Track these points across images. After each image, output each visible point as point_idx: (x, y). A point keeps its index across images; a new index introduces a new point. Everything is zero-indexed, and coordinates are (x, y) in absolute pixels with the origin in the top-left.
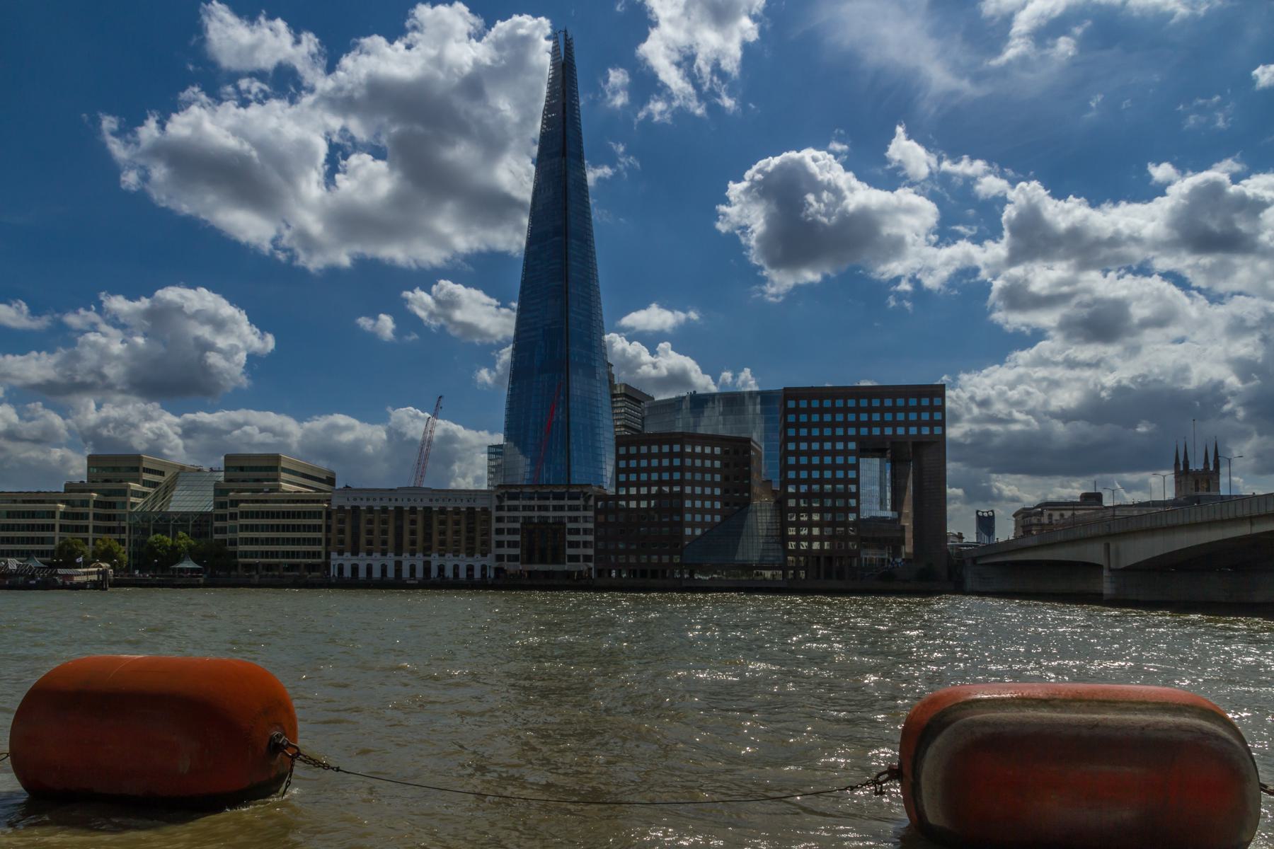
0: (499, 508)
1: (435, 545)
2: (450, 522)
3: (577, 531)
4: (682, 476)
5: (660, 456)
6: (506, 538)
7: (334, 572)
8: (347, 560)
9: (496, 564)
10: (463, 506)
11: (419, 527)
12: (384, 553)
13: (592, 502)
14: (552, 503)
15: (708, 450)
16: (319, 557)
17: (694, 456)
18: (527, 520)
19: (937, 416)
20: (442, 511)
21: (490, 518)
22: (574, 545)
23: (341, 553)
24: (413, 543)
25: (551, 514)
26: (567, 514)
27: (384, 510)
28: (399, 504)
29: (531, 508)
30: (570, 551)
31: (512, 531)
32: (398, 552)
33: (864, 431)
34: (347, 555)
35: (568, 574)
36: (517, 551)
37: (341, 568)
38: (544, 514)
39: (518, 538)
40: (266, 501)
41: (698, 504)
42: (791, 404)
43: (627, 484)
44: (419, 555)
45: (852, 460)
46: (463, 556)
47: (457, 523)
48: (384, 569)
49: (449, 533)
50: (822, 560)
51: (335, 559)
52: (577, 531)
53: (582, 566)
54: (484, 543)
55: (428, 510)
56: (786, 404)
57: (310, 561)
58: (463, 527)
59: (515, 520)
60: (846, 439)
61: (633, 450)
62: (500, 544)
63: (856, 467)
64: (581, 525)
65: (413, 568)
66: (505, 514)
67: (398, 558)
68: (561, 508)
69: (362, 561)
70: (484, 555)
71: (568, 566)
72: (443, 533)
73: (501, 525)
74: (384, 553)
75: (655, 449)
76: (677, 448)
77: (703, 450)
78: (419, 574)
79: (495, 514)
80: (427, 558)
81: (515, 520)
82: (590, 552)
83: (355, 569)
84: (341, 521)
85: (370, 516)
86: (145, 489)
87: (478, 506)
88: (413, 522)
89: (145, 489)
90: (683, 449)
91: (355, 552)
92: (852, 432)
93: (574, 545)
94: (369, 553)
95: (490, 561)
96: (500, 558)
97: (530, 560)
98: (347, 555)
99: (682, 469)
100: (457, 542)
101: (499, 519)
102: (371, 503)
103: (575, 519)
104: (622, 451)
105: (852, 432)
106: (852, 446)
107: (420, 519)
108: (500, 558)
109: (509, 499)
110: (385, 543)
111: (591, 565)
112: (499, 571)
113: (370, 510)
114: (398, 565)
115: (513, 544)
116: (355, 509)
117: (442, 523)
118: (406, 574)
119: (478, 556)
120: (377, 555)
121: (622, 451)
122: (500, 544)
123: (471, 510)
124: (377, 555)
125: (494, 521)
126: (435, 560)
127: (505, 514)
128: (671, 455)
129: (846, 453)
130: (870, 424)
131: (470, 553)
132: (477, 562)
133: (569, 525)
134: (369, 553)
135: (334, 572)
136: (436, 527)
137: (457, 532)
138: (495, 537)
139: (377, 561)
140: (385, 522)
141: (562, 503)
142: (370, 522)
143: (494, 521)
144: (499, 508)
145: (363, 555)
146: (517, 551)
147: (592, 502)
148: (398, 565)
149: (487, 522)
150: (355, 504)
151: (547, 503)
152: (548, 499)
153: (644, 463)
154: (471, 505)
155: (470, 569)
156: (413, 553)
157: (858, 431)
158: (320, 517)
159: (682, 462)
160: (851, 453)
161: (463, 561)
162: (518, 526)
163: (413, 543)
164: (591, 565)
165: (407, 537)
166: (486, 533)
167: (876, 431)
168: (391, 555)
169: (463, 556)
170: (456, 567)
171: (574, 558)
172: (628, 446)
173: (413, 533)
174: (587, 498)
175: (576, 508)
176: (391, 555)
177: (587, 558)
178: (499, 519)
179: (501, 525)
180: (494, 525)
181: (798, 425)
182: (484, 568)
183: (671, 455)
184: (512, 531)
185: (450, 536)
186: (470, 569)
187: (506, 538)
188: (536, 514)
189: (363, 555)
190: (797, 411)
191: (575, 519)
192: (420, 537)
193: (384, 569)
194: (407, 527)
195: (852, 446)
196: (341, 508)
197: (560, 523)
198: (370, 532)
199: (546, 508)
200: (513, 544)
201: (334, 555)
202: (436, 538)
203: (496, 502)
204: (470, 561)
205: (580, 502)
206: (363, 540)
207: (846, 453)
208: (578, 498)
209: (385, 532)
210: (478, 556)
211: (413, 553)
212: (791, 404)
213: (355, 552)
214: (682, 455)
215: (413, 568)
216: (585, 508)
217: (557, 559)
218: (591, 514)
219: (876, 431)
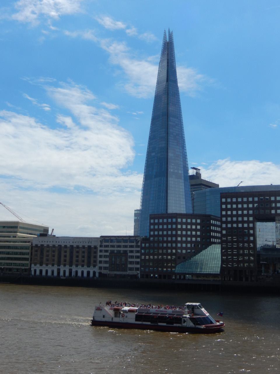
0: (101, 246)
1: (74, 262)
2: (81, 252)
3: (132, 257)
4: (176, 232)
5: (167, 224)
6: (103, 259)
7: (33, 273)
8: (38, 268)
9: (99, 271)
10: (86, 245)
11: (68, 254)
12: (53, 265)
13: (139, 244)
14: (123, 244)
15: (194, 221)
16: (28, 266)
17: (182, 223)
18: (112, 252)
20: (78, 247)
21: (97, 250)
22: (131, 263)
23: (35, 265)
24: (65, 261)
25: (122, 249)
26: (129, 249)
27: (54, 246)
28: (60, 244)
29: (113, 246)
30: (129, 266)
31: (105, 256)
32: (59, 265)
34: (38, 265)
35: (128, 275)
36: (107, 265)
37: (35, 271)
39: (108, 259)
40: (10, 242)
41: (184, 245)
42: (224, 200)
45: (251, 225)
46: (85, 266)
47: (84, 252)
48: (53, 272)
49: (80, 257)
50: (134, 268)
51: (33, 267)
52: (132, 257)
53: (134, 272)
54: (95, 261)
55: (72, 247)
56: (221, 200)
57: (23, 268)
58: (86, 255)
59: (106, 251)
60: (248, 215)
61: (156, 221)
62: (100, 262)
63: (254, 228)
65: (65, 272)
66: (103, 249)
67: (59, 267)
68: (126, 246)
69: (44, 268)
70: (94, 266)
71: (129, 272)
72: (77, 257)
73: (101, 254)
74: (53, 265)
76: (174, 220)
77: (187, 221)
78: (67, 274)
79: (99, 249)
80: (71, 268)
81: (106, 251)
82: (139, 266)
83: (41, 271)
84: (36, 251)
85: (48, 249)
87: (93, 245)
88: (66, 252)
90: (177, 220)
91: (41, 265)
93: (131, 263)
94: (47, 265)
96: (100, 268)
98: (38, 265)
100: (83, 261)
101: (101, 251)
102: (48, 243)
103: (132, 252)
104: (152, 221)
106: (251, 219)
107: (68, 250)
108: (100, 268)
109: (105, 242)
110: (54, 260)
111: (139, 272)
112: (100, 274)
113: (48, 246)
114: (59, 270)
115: (106, 262)
116: (42, 245)
117: (78, 252)
118: (62, 274)
119: (92, 267)
120: (50, 266)
121: (152, 221)
122: (100, 262)
123: (89, 247)
124: (50, 266)
125: (99, 251)
126: (74, 269)
127: (103, 249)
128: (172, 223)
129: (248, 222)
131: (89, 266)
133: (129, 254)
134: (47, 265)
135: (33, 273)
136: (75, 254)
137: (83, 257)
138: (99, 259)
139: (50, 268)
140: (54, 252)
141: (126, 244)
142: (48, 251)
143: (99, 251)
144: (101, 246)
145: (44, 265)
146: (107, 265)
147: (139, 244)
148: (59, 270)
149: (96, 252)
150: (42, 244)
151: (120, 244)
152: (121, 242)
153: (161, 227)
154: (90, 244)
155: (88, 273)
156: (65, 265)
158: (29, 249)
160: (251, 222)
161: (86, 270)
162: (108, 254)
163: (65, 261)
165: (62, 258)
166: (95, 257)
168: (56, 266)
169: (85, 266)
170: (83, 272)
171: (131, 269)
172: (154, 218)
173: (65, 256)
174: (137, 242)
175: (131, 246)
176: (56, 266)
177: (137, 269)
178: (101, 251)
179: (101, 254)
180: (99, 254)
181: (227, 210)
182: (94, 273)
183: (172, 223)
184: (105, 256)
185: (80, 258)
186: (88, 273)
187: (103, 259)
188: (116, 249)
189: (44, 265)
190: (226, 203)
191: (132, 252)
192: (68, 259)
193: (53, 272)
194: (63, 254)
196: (36, 246)
197: (125, 252)
198: (48, 256)
199: (119, 246)
200: (106, 262)
201: (33, 265)
202: (74, 258)
203: (99, 244)
204: (89, 269)
205: (134, 244)
206: (45, 259)
207: (248, 222)
208: (133, 242)
209: (54, 256)
210: (92, 267)
211: (65, 265)
212: (224, 200)
213: (41, 265)
214: (176, 223)
215: (65, 272)
216: (137, 246)
218: (139, 249)
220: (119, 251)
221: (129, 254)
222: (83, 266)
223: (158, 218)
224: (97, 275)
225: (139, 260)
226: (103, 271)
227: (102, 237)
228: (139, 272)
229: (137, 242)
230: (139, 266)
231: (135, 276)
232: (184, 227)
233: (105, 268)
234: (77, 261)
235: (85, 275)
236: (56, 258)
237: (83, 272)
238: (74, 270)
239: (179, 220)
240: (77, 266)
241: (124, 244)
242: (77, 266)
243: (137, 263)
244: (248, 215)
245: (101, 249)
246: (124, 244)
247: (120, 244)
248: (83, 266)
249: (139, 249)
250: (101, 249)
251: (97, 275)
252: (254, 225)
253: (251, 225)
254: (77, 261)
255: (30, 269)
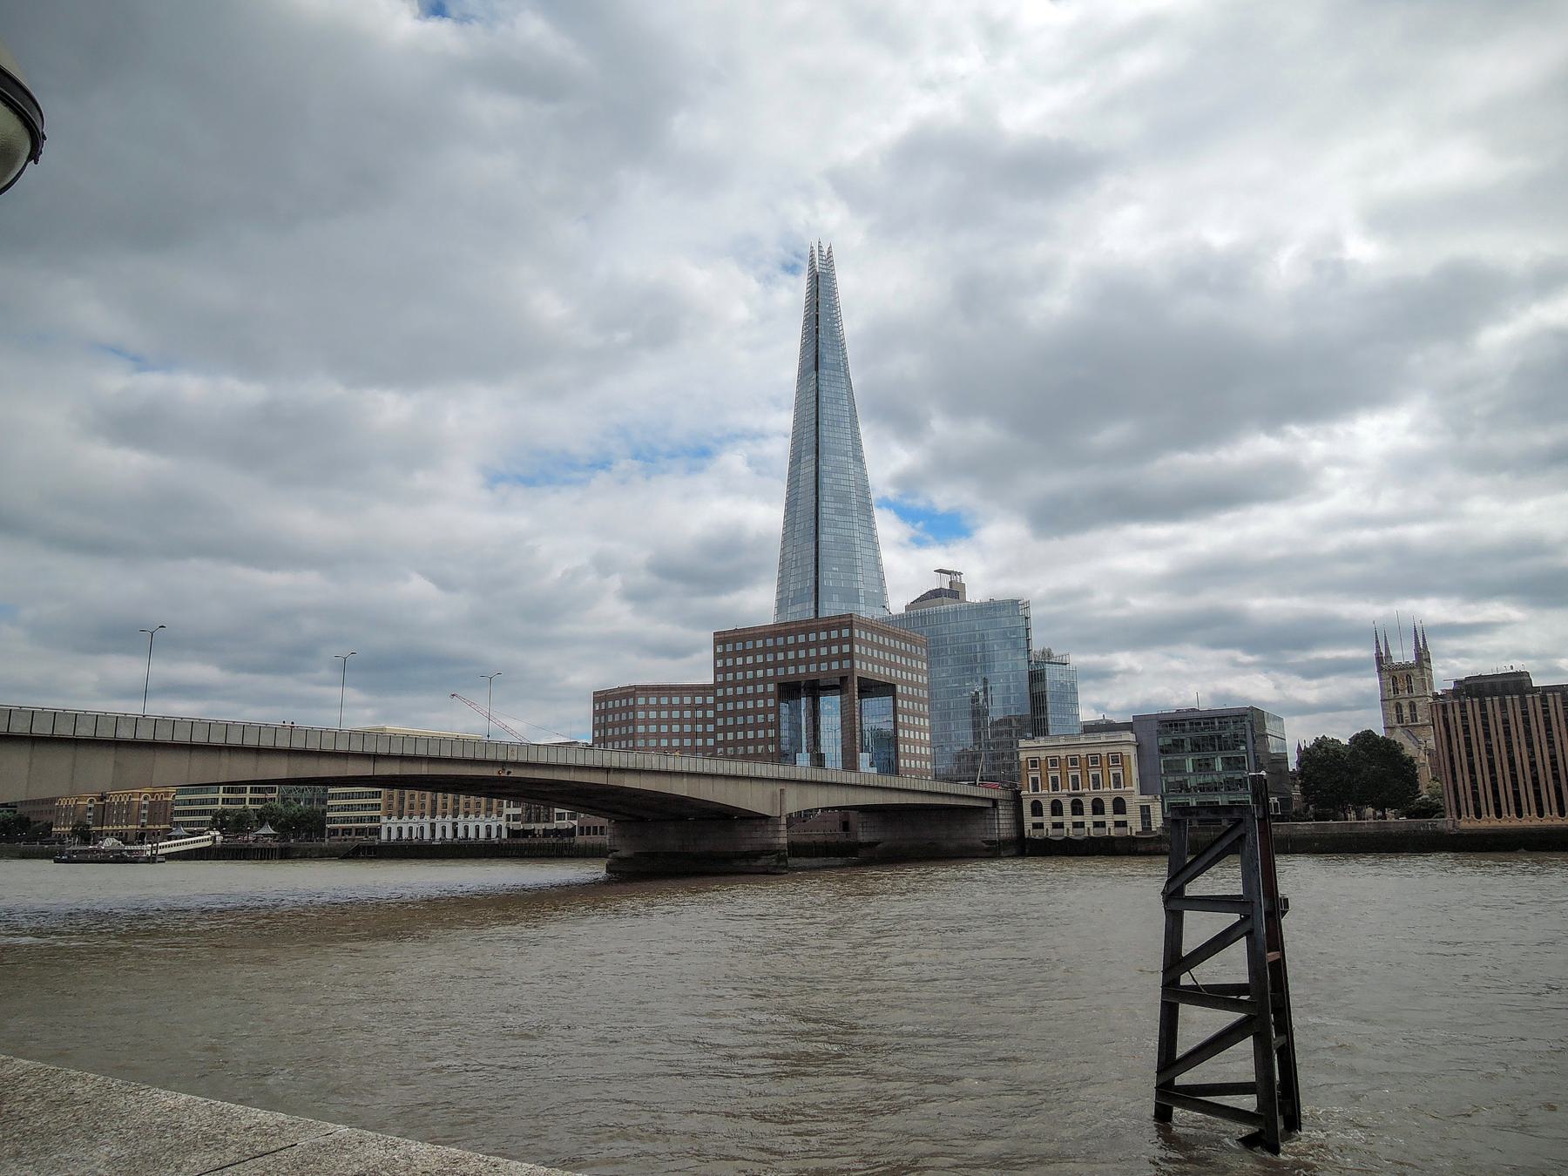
19: (846, 648)
23: (390, 817)
33: (781, 672)
34: (394, 819)
44: (449, 817)
95: (504, 824)
97: (529, 821)
105: (770, 672)
106: (771, 688)
114: (433, 825)
120: (416, 818)
124: (416, 818)
130: (785, 664)
132: (495, 822)
135: (384, 836)
145: (406, 818)
148: (433, 825)
160: (770, 696)
167: (791, 670)
169: (482, 816)
170: (477, 829)
182: (499, 828)
201: (384, 819)
207: (765, 695)
217: (548, 820)
219: (791, 670)
222: (477, 814)
224: (504, 835)
226: (518, 825)
232: (653, 715)
235: (482, 835)
237: (477, 829)
240: (467, 814)
244: (765, 680)
248: (477, 814)
255: (377, 831)
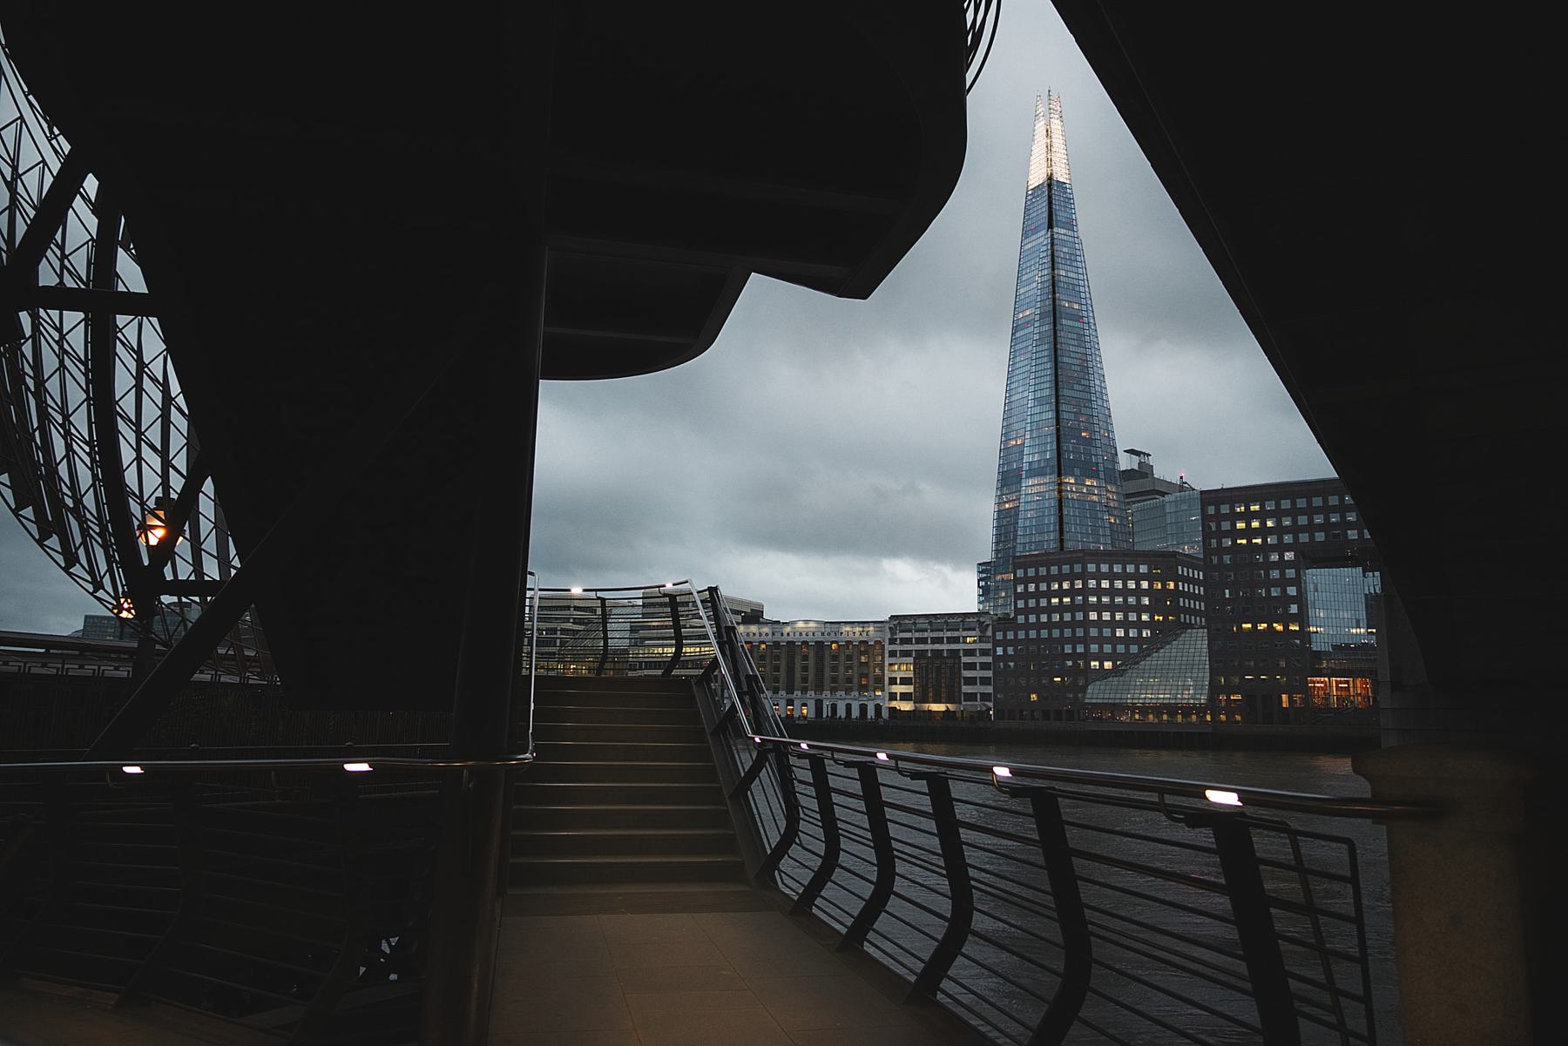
0: (892, 641)
1: (827, 681)
3: (971, 666)
11: (811, 663)
13: (989, 633)
22: (971, 681)
24: (805, 680)
25: (945, 647)
29: (923, 641)
30: (966, 689)
33: (1304, 538)
36: (909, 689)
38: (937, 646)
43: (1026, 611)
45: (1291, 573)
49: (842, 669)
52: (971, 666)
53: (978, 705)
55: (820, 644)
61: (1031, 572)
63: (1298, 582)
64: (978, 659)
66: (897, 648)
72: (834, 669)
75: (1043, 571)
79: (888, 648)
82: (990, 689)
86: (576, 627)
88: (805, 658)
89: (576, 627)
90: (1084, 568)
92: (1288, 539)
93: (971, 681)
99: (1085, 592)
110: (777, 680)
127: (897, 648)
133: (965, 660)
140: (777, 658)
141: (956, 634)
144: (892, 641)
146: (909, 689)
147: (989, 633)
151: (941, 634)
155: (863, 708)
157: (1296, 538)
159: (1085, 584)
160: (1290, 564)
163: (805, 680)
164: (991, 705)
165: (798, 675)
170: (849, 707)
171: (971, 697)
173: (805, 669)
177: (985, 697)
186: (863, 708)
194: (798, 664)
195: (1289, 556)
197: (954, 654)
202: (828, 673)
220: (938, 653)
221: (965, 660)
223: (1037, 566)
224: (885, 714)
225: (989, 674)
227: (892, 617)
228: (991, 705)
229: (983, 628)
230: (990, 689)
231: (983, 715)
233: (905, 697)
234: (834, 680)
235: (855, 713)
236: (782, 674)
237: (849, 707)
238: (826, 703)
239: (1091, 568)
240: (833, 690)
241: (949, 634)
242: (833, 690)
243: (985, 681)
245: (893, 647)
246: (949, 634)
247: (941, 634)
249: (990, 646)
250: (893, 647)
251: (885, 714)
252: (1298, 573)
253: (1291, 573)
254: (834, 680)
